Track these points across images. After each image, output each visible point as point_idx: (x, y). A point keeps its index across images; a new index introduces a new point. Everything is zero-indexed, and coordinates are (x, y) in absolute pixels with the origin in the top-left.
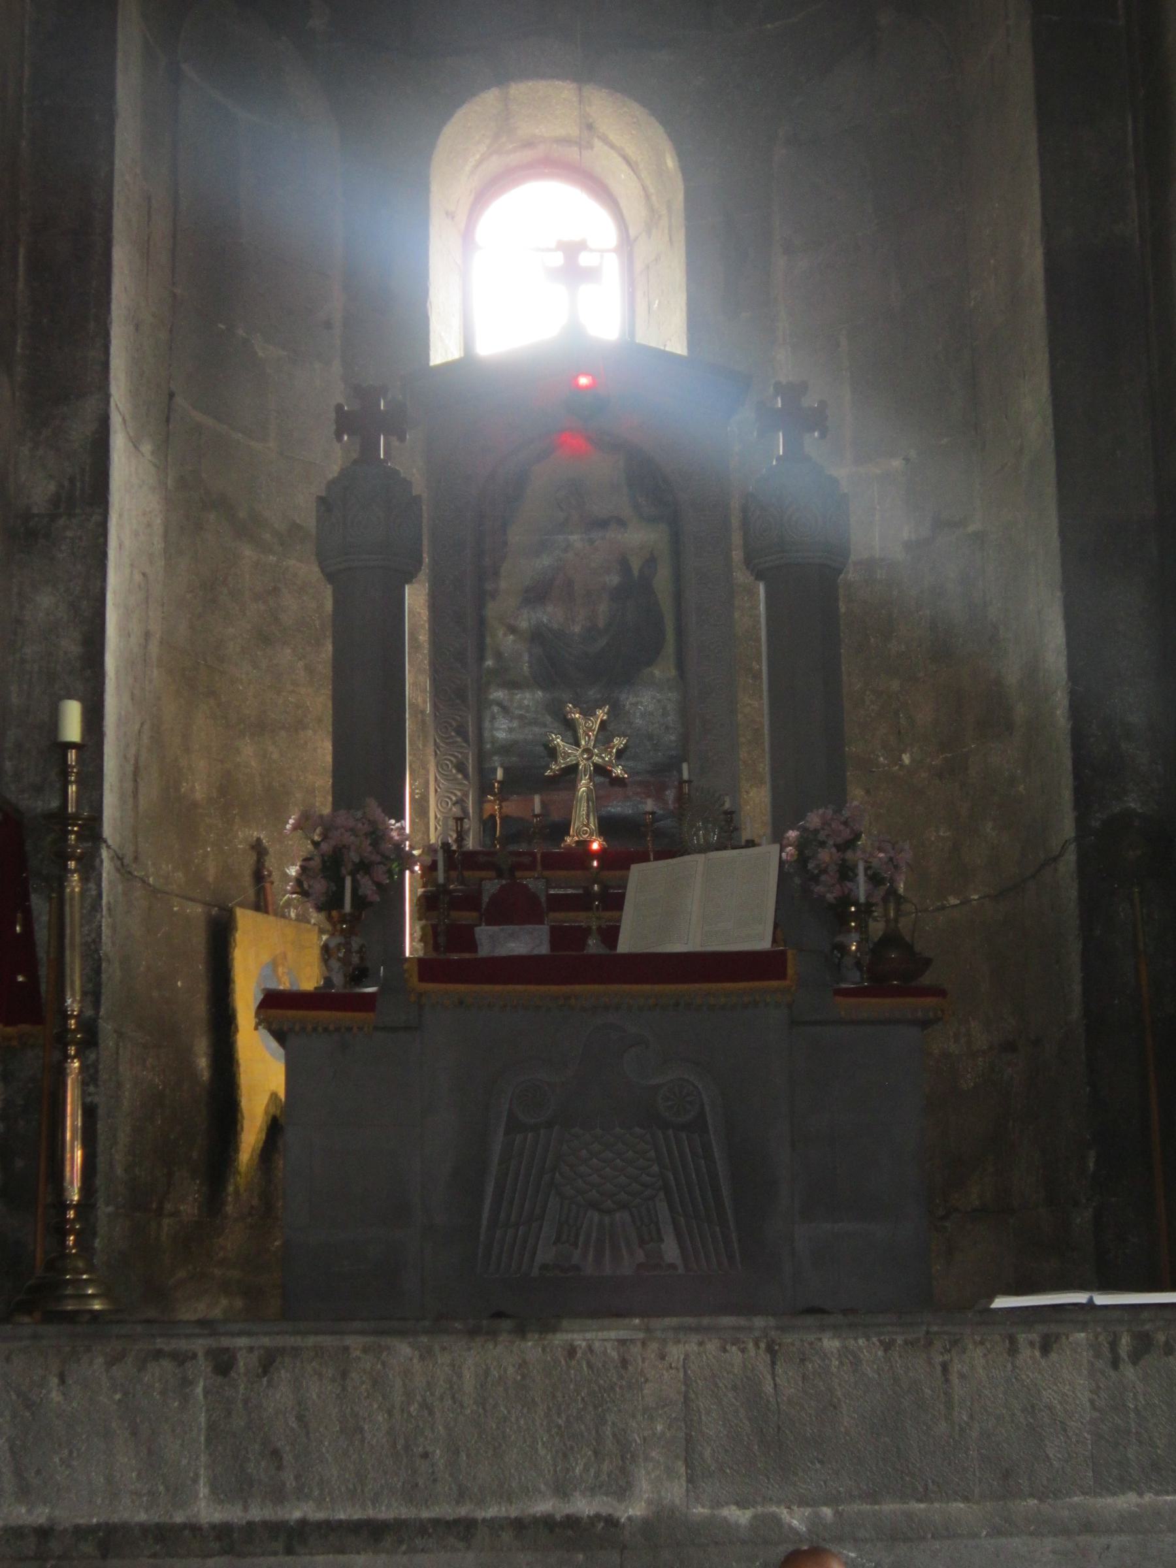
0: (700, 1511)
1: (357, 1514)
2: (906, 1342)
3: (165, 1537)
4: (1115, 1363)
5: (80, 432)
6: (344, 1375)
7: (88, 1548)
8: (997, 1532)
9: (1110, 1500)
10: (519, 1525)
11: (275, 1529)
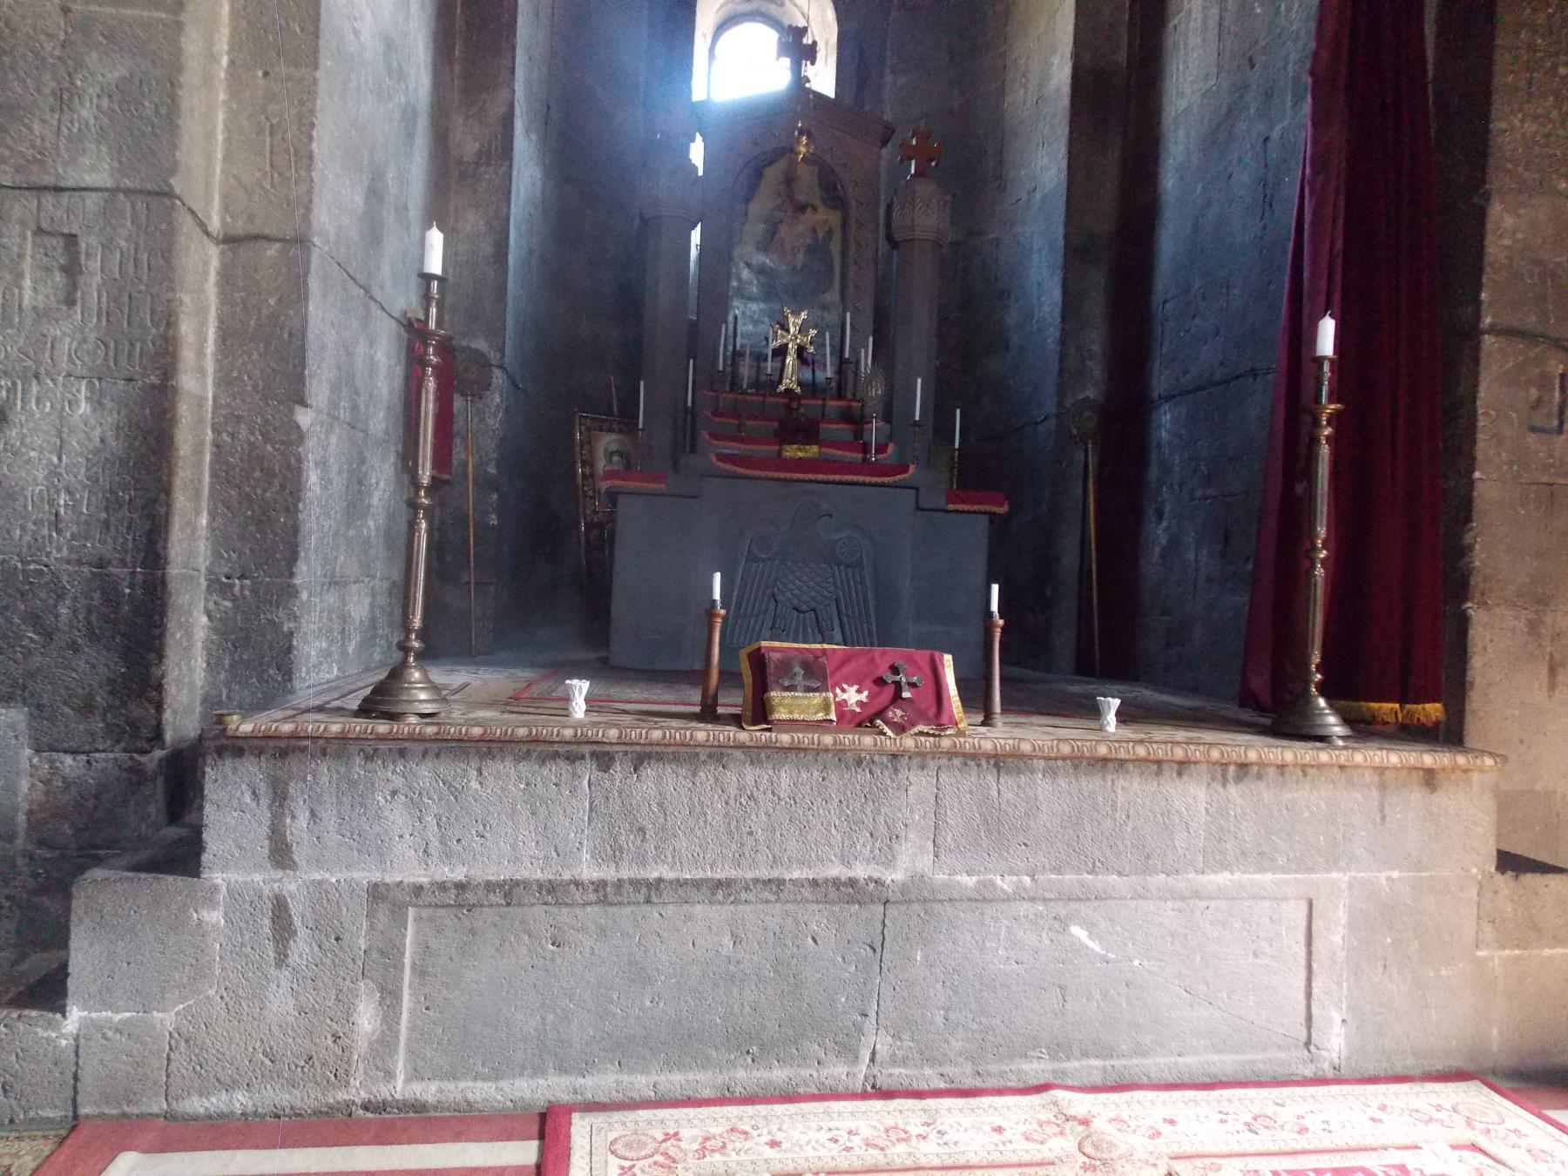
0: (941, 877)
1: (699, 875)
5: (496, 110)
7: (497, 898)
8: (1138, 897)
9: (1212, 877)
10: (814, 883)
11: (635, 883)
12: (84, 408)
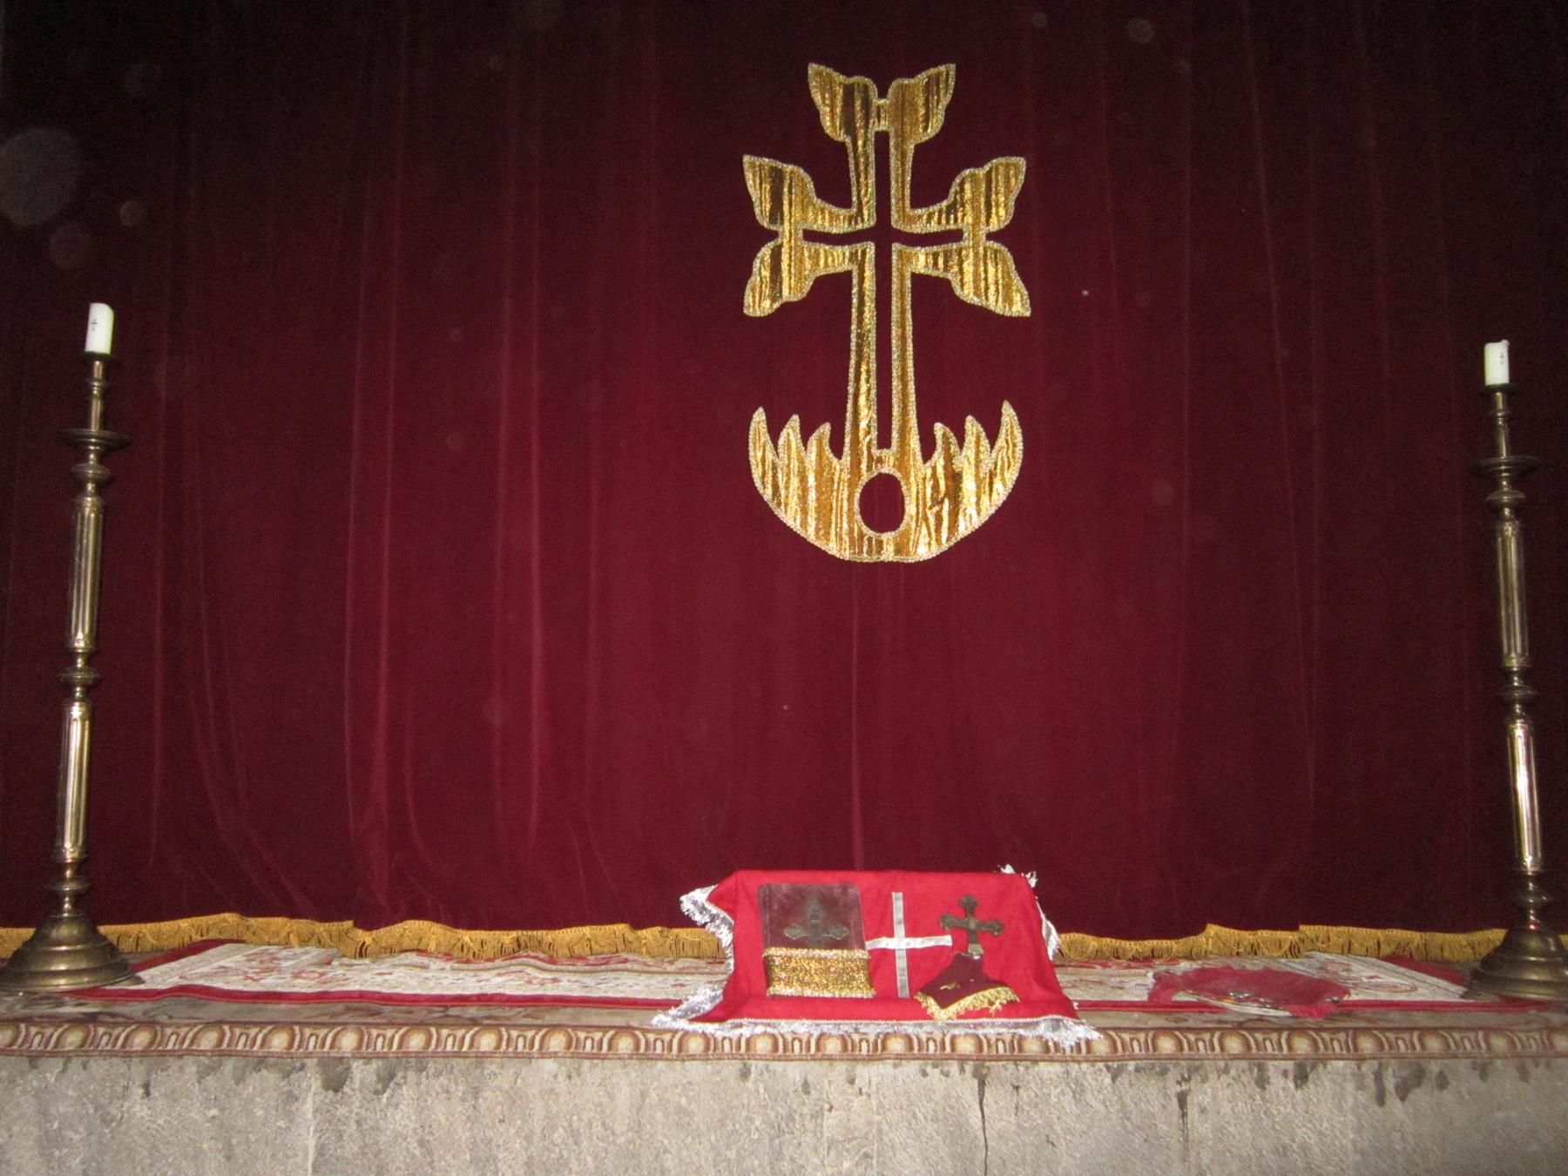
2: (1137, 1070)
4: (1381, 1098)
6: (476, 1092)
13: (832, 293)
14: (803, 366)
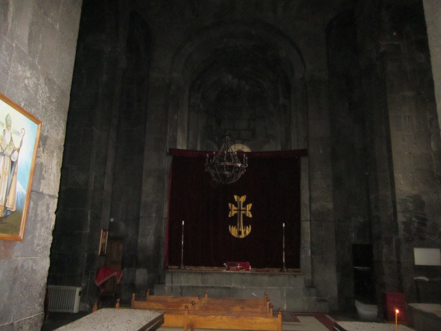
3: (197, 287)
12: (153, 238)
13: (236, 215)
14: (234, 221)
